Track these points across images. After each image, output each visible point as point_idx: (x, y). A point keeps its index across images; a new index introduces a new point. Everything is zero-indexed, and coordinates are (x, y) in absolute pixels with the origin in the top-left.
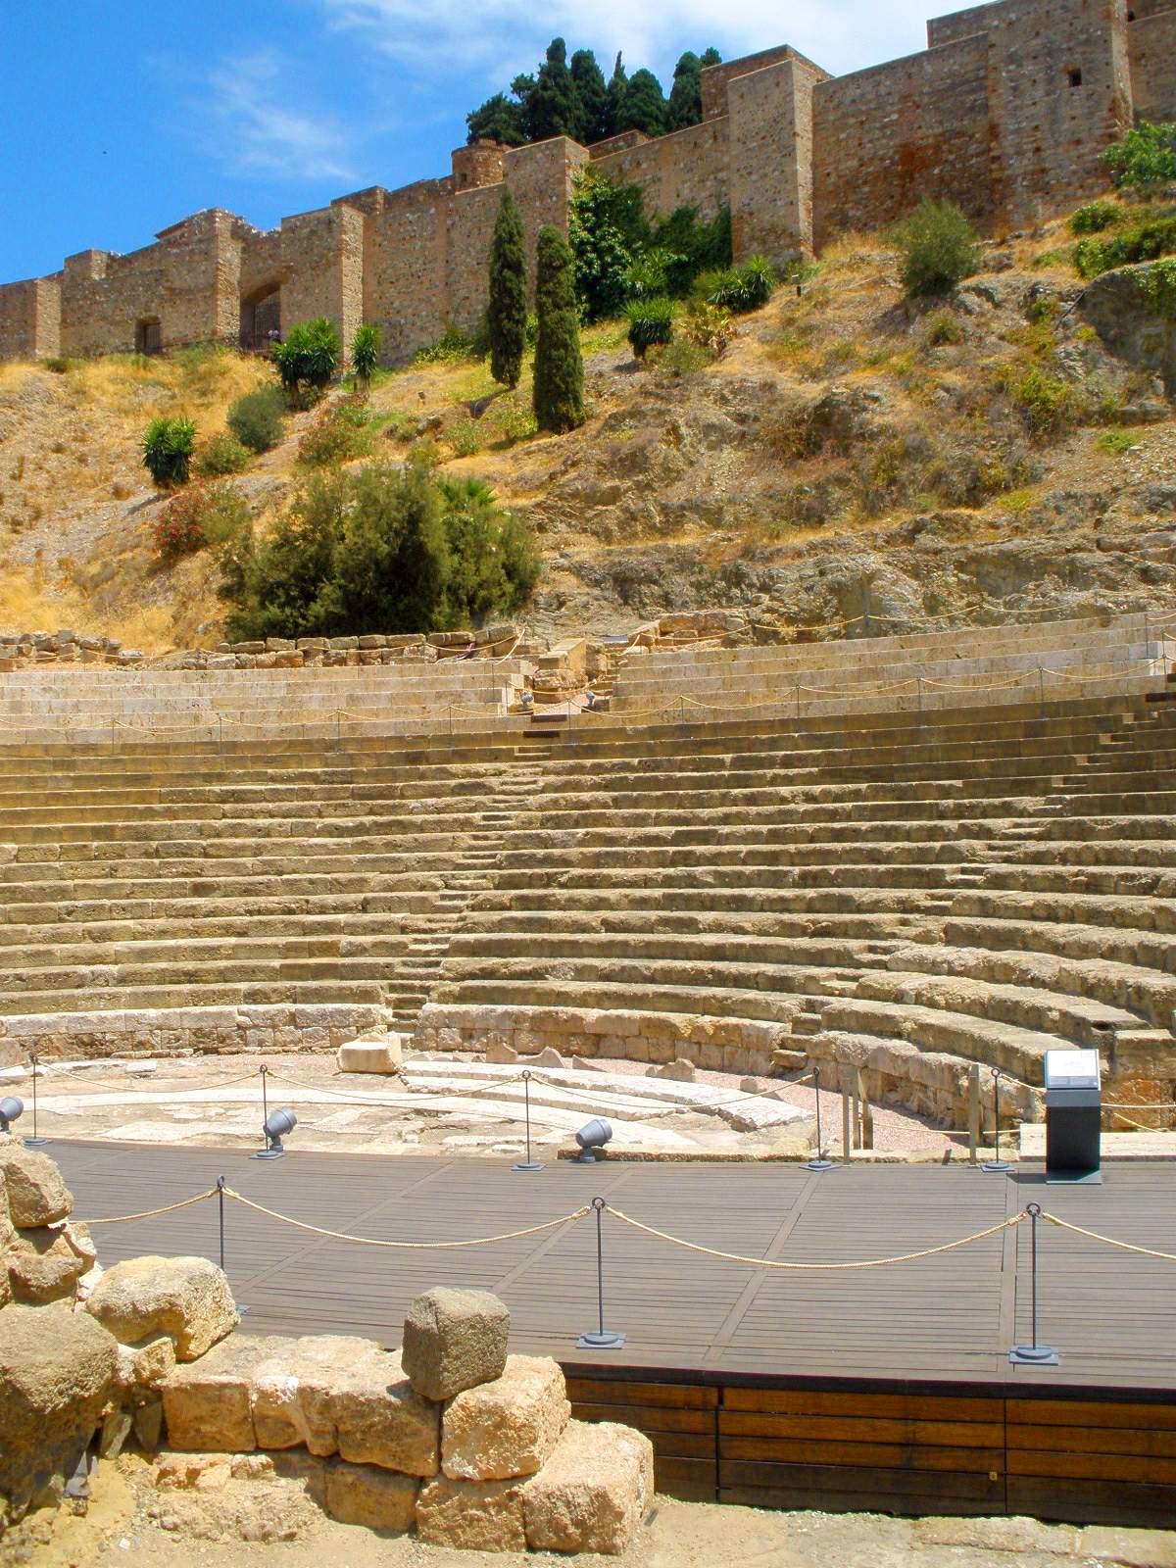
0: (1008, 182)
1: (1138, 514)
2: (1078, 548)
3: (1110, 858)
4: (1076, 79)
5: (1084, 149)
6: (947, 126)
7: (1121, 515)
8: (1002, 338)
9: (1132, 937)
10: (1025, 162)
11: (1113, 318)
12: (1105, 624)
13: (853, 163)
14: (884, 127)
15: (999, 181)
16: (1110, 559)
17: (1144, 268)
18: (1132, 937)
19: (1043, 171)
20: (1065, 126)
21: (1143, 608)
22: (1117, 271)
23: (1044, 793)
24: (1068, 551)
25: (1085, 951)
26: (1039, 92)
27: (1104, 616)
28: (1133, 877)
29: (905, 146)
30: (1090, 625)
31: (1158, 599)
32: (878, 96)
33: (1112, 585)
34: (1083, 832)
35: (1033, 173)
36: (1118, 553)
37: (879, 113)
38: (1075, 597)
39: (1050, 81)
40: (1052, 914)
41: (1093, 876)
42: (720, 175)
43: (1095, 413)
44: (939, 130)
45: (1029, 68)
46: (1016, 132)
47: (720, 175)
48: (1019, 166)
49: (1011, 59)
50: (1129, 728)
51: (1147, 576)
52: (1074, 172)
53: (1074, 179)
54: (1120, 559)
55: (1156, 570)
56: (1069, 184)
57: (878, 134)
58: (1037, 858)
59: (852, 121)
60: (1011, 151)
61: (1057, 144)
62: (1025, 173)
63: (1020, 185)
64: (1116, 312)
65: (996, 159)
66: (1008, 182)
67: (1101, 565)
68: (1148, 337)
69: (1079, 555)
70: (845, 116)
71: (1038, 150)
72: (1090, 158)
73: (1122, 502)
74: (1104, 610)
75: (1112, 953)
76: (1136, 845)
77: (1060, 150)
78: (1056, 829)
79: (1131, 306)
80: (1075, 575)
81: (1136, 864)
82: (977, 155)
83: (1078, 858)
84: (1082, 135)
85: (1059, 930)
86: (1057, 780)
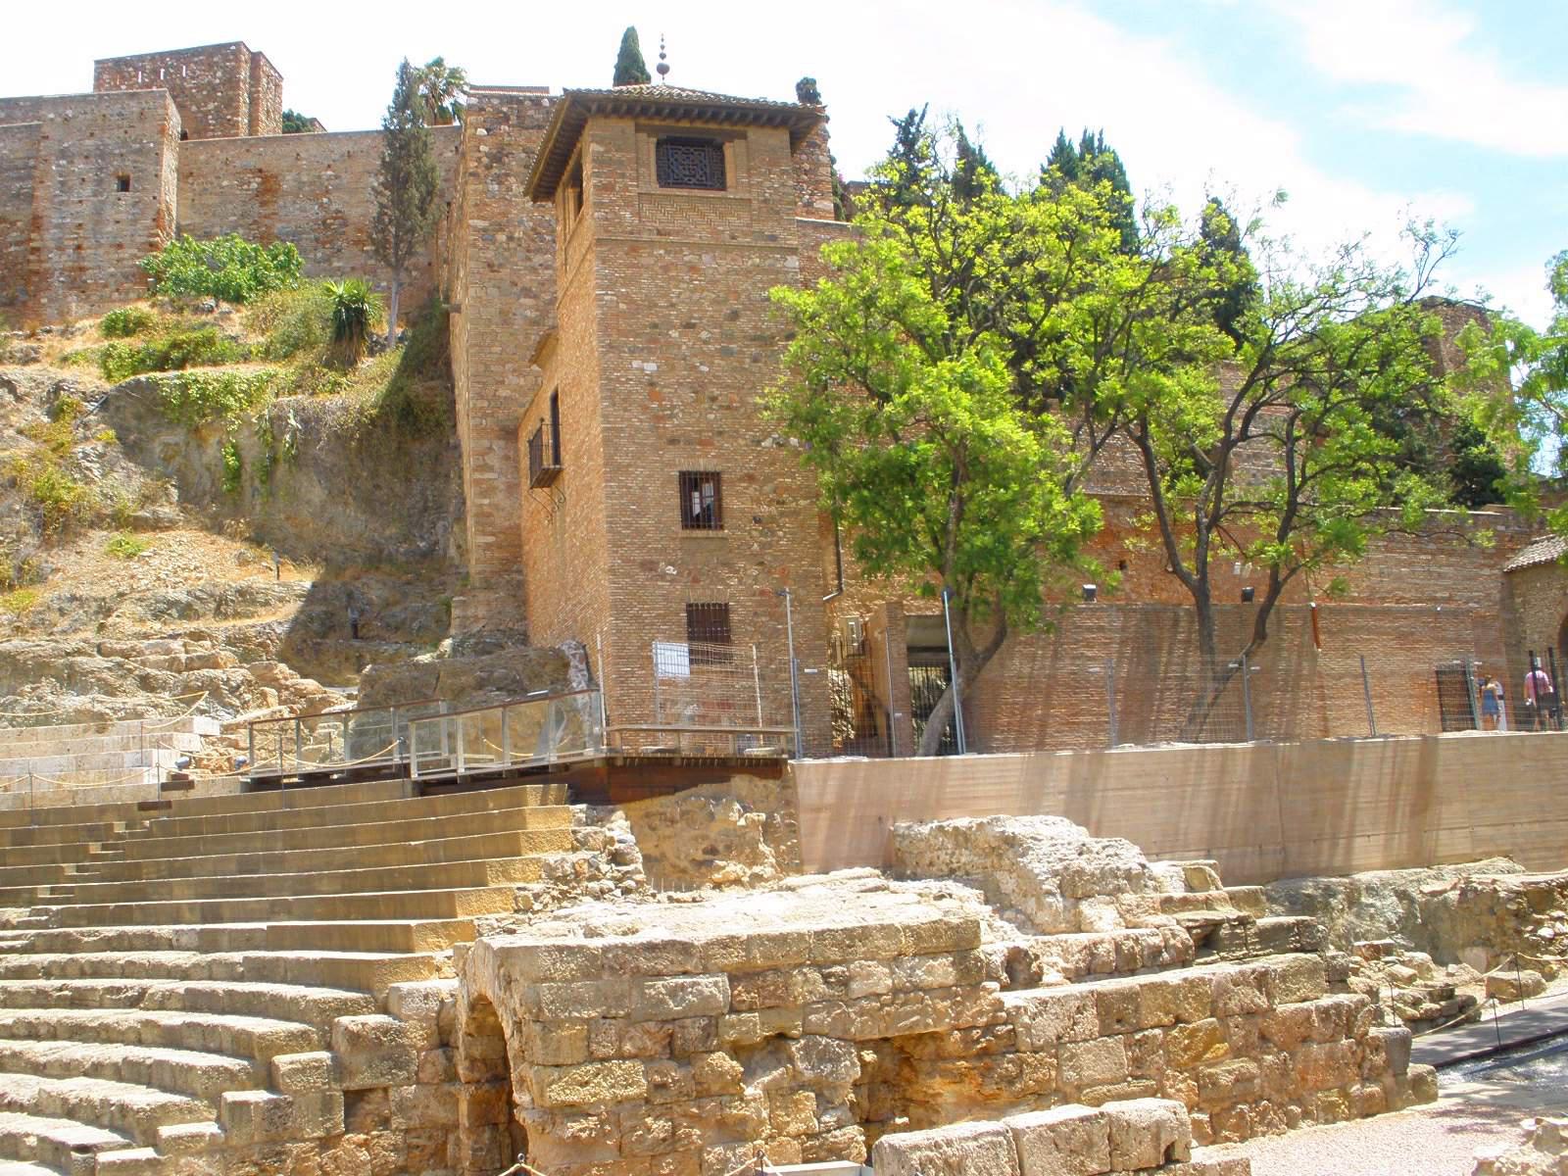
1: (142, 621)
2: (79, 652)
3: (97, 970)
4: (124, 185)
5: (125, 253)
7: (126, 621)
8: (20, 432)
9: (116, 1053)
10: (64, 258)
11: (134, 423)
12: (101, 730)
15: (37, 273)
16: (110, 665)
17: (169, 377)
18: (116, 1053)
19: (82, 269)
20: (109, 229)
21: (140, 716)
22: (142, 377)
23: (30, 903)
24: (68, 654)
25: (67, 1069)
26: (87, 191)
27: (101, 722)
28: (119, 990)
30: (85, 731)
31: (156, 706)
33: (110, 691)
34: (69, 945)
35: (72, 269)
36: (119, 659)
38: (72, 701)
39: (100, 182)
40: (33, 1032)
41: (77, 989)
43: (108, 516)
45: (80, 166)
46: (57, 226)
49: (63, 154)
50: (120, 837)
51: (146, 683)
52: (112, 275)
53: (112, 281)
54: (120, 665)
55: (155, 678)
56: (105, 286)
58: (19, 973)
60: (51, 244)
61: (99, 245)
62: (63, 269)
63: (57, 280)
64: (139, 417)
65: (37, 249)
67: (101, 670)
68: (167, 445)
69: (79, 659)
71: (79, 247)
72: (130, 263)
73: (127, 607)
74: (101, 716)
75: (96, 1070)
76: (122, 957)
77: (101, 251)
78: (40, 943)
79: (155, 414)
80: (72, 679)
81: (123, 976)
82: (17, 244)
83: (63, 971)
84: (126, 241)
85: (39, 1050)
86: (43, 891)
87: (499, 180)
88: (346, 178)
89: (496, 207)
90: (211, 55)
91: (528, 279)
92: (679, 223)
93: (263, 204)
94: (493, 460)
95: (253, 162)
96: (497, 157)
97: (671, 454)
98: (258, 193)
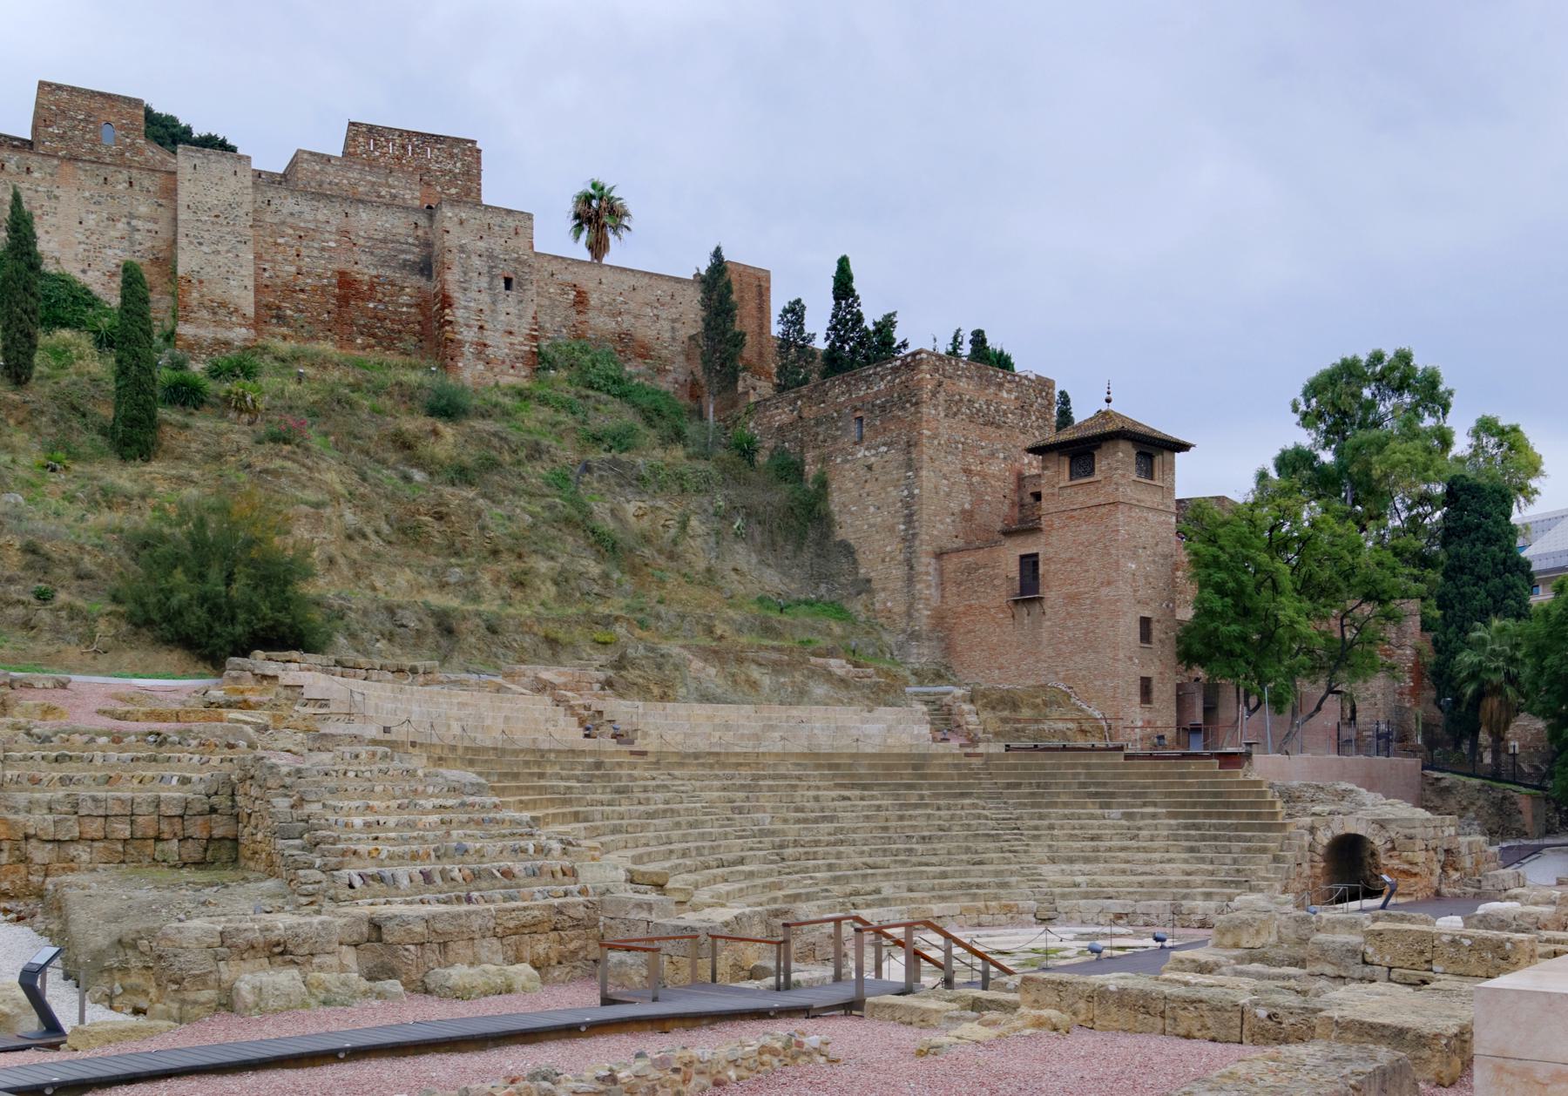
0: (460, 344)
4: (508, 283)
6: (381, 271)
13: (293, 269)
14: (323, 249)
29: (342, 274)
32: (316, 221)
35: (478, 344)
37: (318, 235)
42: (134, 222)
44: (375, 273)
45: (476, 261)
46: (465, 307)
47: (134, 222)
48: (468, 335)
49: (462, 249)
57: (316, 253)
59: (291, 231)
66: (460, 344)
70: (283, 223)
71: (481, 327)
82: (410, 306)
84: (514, 329)
87: (936, 407)
88: (632, 305)
89: (934, 424)
90: (451, 146)
91: (945, 469)
92: (1142, 497)
93: (579, 312)
94: (931, 569)
95: (569, 278)
96: (934, 394)
97: (1138, 608)
98: (575, 303)
